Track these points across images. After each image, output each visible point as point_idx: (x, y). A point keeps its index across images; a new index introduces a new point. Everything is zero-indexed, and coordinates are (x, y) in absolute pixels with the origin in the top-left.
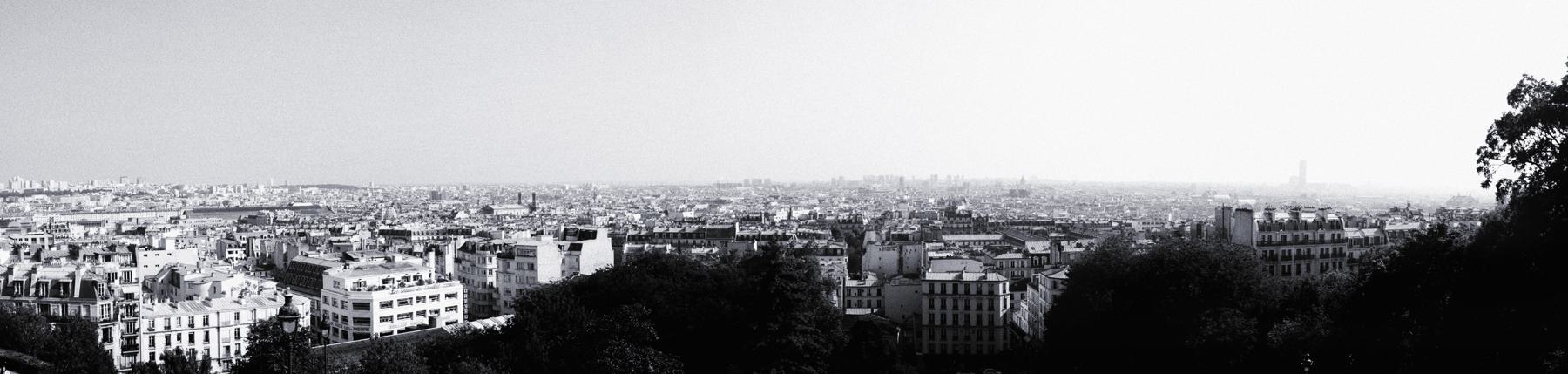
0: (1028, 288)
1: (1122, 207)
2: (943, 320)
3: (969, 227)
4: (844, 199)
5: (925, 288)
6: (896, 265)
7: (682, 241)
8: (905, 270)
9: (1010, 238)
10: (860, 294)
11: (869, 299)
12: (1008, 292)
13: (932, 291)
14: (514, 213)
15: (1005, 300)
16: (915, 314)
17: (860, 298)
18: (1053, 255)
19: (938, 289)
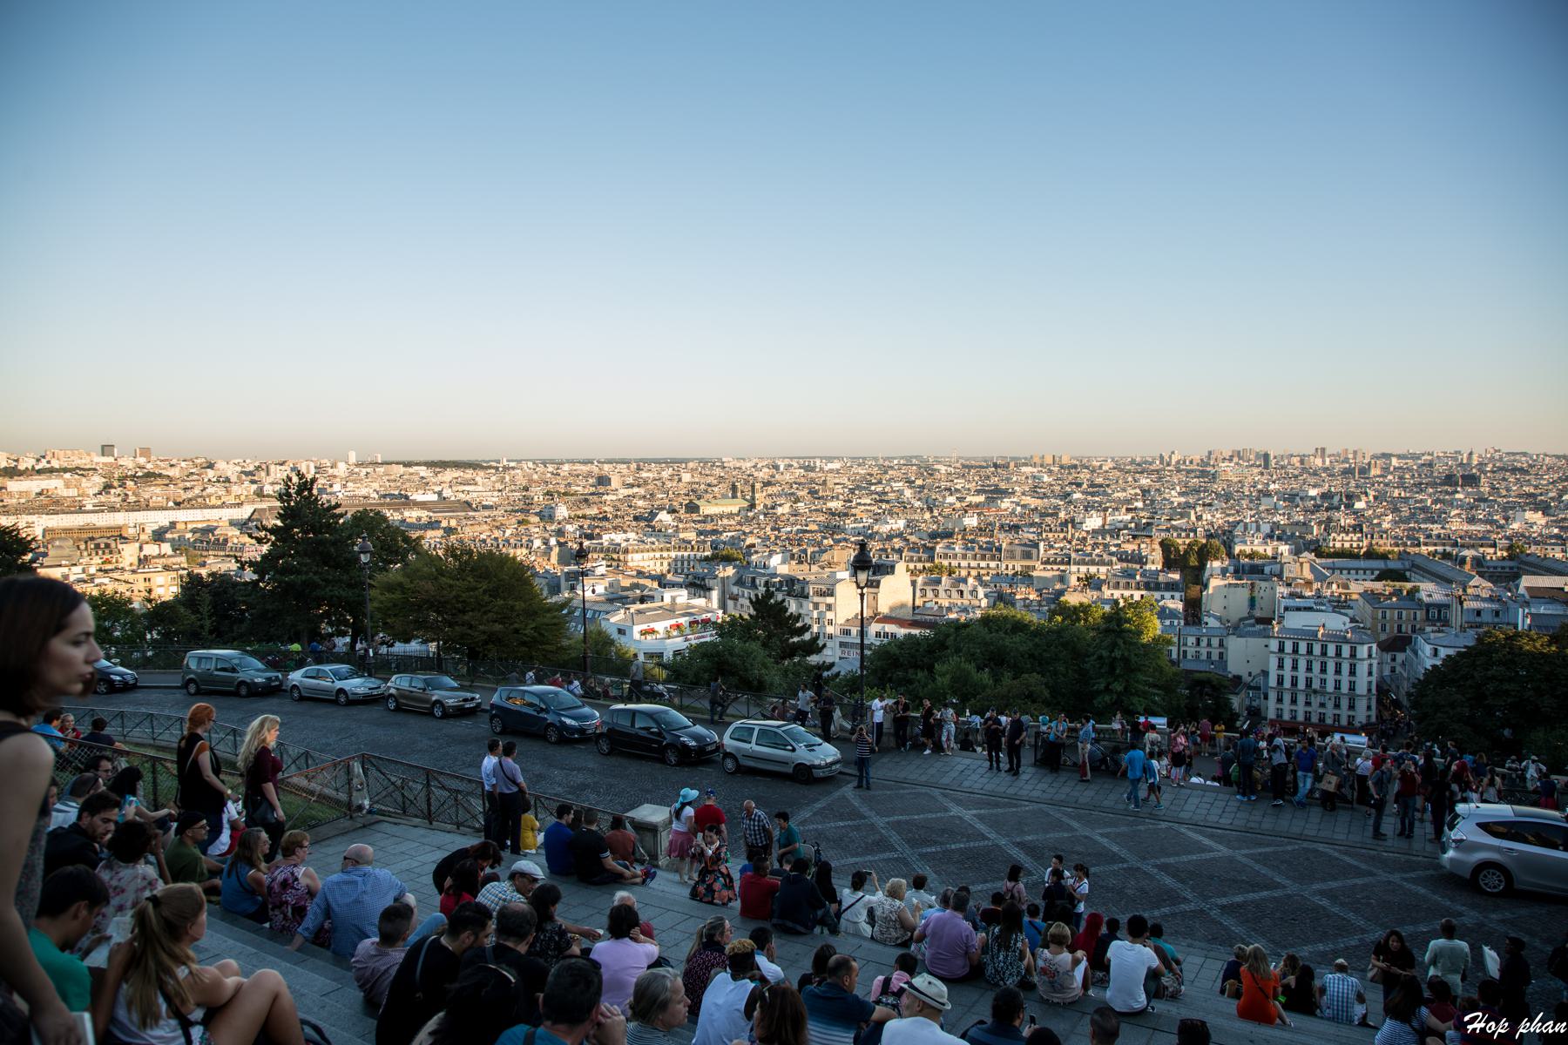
2: (1294, 682)
3: (1359, 548)
4: (1178, 488)
5: (1274, 645)
6: (1246, 603)
7: (974, 564)
8: (1258, 613)
9: (1419, 567)
10: (1198, 644)
12: (1374, 655)
13: (1281, 650)
14: (727, 510)
15: (1371, 665)
16: (1263, 671)
17: (1198, 649)
19: (1288, 647)
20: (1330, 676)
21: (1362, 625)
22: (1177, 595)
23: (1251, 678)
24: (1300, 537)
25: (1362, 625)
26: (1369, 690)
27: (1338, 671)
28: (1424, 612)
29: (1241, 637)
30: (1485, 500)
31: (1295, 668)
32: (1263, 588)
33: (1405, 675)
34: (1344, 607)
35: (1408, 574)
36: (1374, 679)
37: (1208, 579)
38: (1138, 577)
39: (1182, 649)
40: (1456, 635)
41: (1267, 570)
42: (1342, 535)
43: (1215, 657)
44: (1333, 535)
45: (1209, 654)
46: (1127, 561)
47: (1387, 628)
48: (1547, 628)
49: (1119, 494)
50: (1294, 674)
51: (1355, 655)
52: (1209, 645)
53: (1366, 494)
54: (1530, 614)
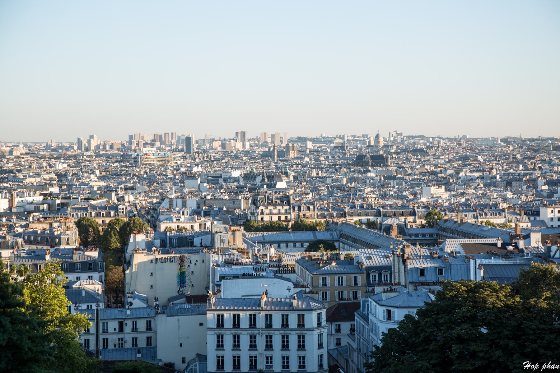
0: (356, 318)
1: (536, 181)
3: (287, 220)
4: (98, 172)
8: (188, 291)
9: (346, 237)
10: (121, 329)
11: (134, 335)
12: (324, 323)
15: (321, 335)
16: (198, 355)
17: (121, 336)
18: (397, 271)
20: (277, 353)
21: (307, 290)
22: (96, 275)
23: (186, 365)
24: (228, 212)
25: (307, 290)
26: (321, 366)
27: (285, 346)
28: (365, 275)
29: (172, 316)
30: (394, 178)
31: (236, 346)
32: (193, 262)
33: (355, 346)
34: (286, 272)
35: (336, 244)
36: (324, 351)
37: (131, 256)
38: (48, 257)
39: (101, 337)
40: (409, 294)
41: (197, 241)
42: (270, 208)
43: (142, 343)
44: (261, 208)
45: (135, 340)
46: (38, 243)
47: (329, 296)
48: (508, 279)
49: (32, 180)
50: (236, 353)
51: (303, 325)
52: (135, 329)
53: (287, 175)
54: (484, 265)
